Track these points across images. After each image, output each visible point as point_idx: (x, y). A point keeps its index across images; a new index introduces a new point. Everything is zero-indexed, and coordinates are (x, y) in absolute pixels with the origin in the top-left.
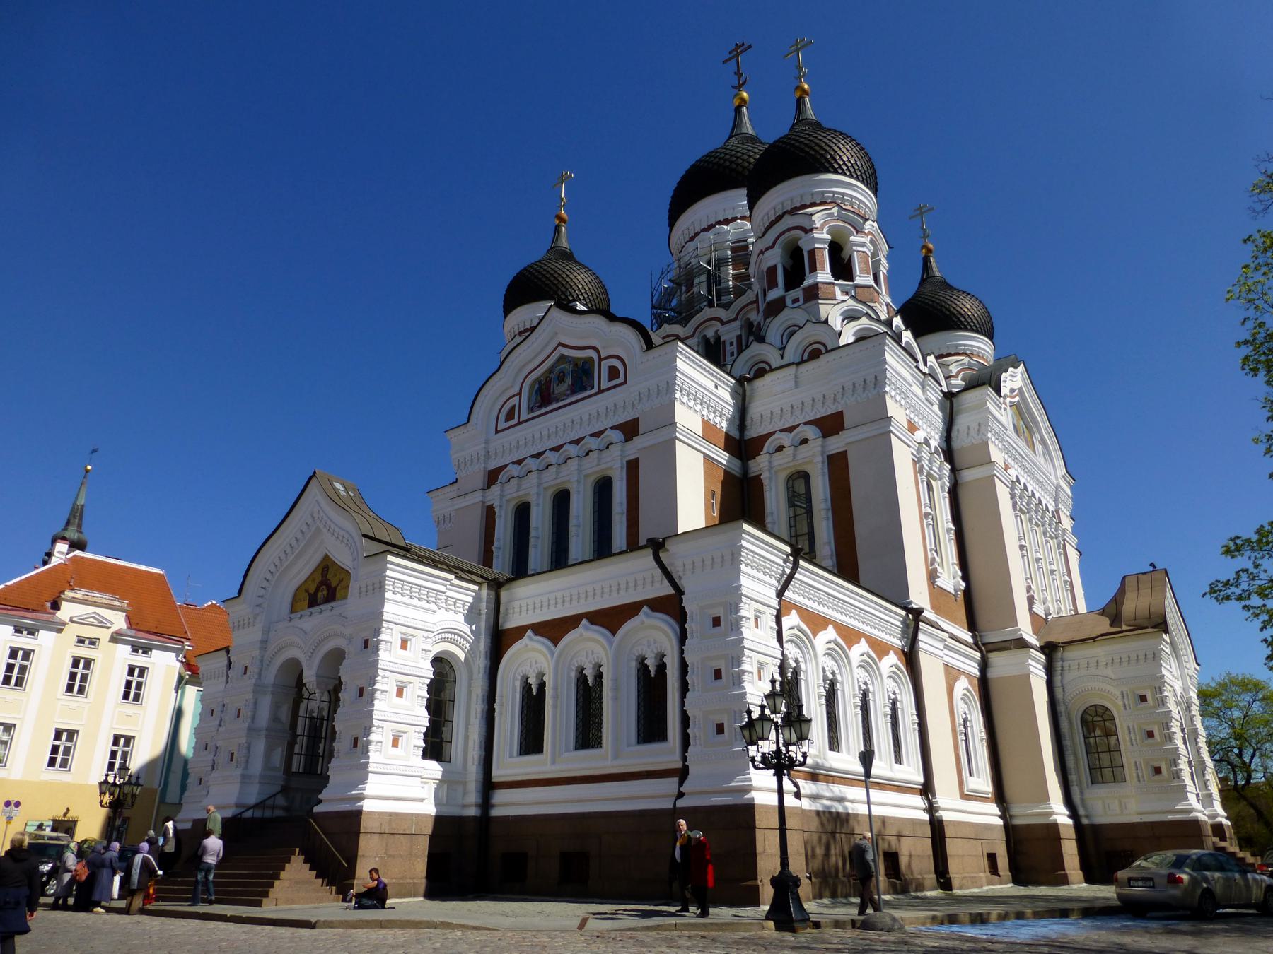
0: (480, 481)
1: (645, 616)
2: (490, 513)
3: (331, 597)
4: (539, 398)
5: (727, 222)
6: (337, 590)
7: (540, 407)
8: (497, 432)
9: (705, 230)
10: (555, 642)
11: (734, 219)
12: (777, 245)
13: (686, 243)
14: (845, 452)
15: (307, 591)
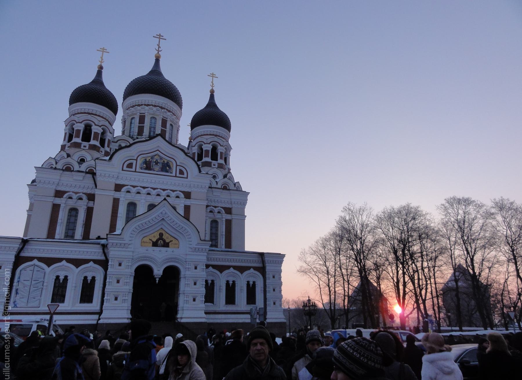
0: (113, 187)
1: (252, 270)
2: (116, 202)
3: (166, 245)
4: (145, 165)
5: (162, 108)
6: (170, 244)
7: (146, 169)
8: (123, 170)
9: (152, 105)
10: (221, 272)
11: (164, 108)
12: (211, 144)
13: (142, 105)
14: (231, 220)
15: (151, 240)
